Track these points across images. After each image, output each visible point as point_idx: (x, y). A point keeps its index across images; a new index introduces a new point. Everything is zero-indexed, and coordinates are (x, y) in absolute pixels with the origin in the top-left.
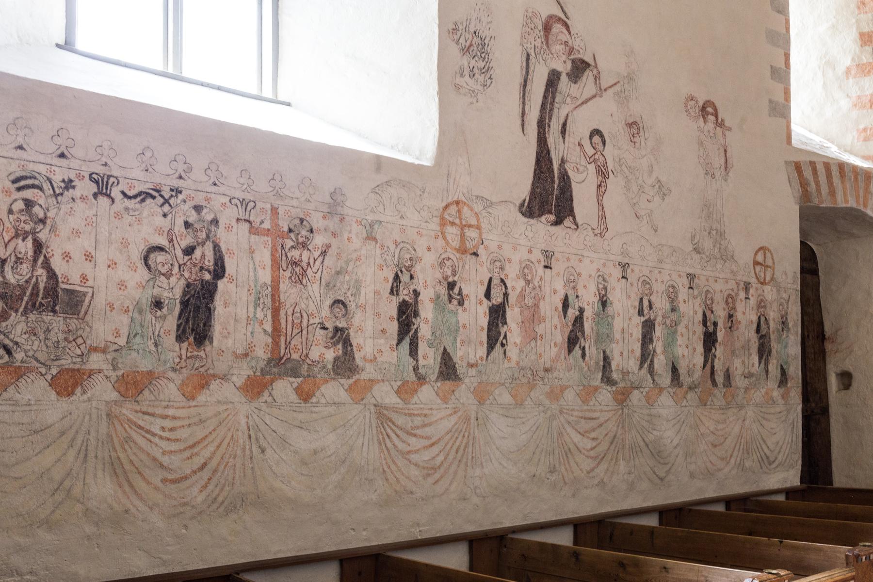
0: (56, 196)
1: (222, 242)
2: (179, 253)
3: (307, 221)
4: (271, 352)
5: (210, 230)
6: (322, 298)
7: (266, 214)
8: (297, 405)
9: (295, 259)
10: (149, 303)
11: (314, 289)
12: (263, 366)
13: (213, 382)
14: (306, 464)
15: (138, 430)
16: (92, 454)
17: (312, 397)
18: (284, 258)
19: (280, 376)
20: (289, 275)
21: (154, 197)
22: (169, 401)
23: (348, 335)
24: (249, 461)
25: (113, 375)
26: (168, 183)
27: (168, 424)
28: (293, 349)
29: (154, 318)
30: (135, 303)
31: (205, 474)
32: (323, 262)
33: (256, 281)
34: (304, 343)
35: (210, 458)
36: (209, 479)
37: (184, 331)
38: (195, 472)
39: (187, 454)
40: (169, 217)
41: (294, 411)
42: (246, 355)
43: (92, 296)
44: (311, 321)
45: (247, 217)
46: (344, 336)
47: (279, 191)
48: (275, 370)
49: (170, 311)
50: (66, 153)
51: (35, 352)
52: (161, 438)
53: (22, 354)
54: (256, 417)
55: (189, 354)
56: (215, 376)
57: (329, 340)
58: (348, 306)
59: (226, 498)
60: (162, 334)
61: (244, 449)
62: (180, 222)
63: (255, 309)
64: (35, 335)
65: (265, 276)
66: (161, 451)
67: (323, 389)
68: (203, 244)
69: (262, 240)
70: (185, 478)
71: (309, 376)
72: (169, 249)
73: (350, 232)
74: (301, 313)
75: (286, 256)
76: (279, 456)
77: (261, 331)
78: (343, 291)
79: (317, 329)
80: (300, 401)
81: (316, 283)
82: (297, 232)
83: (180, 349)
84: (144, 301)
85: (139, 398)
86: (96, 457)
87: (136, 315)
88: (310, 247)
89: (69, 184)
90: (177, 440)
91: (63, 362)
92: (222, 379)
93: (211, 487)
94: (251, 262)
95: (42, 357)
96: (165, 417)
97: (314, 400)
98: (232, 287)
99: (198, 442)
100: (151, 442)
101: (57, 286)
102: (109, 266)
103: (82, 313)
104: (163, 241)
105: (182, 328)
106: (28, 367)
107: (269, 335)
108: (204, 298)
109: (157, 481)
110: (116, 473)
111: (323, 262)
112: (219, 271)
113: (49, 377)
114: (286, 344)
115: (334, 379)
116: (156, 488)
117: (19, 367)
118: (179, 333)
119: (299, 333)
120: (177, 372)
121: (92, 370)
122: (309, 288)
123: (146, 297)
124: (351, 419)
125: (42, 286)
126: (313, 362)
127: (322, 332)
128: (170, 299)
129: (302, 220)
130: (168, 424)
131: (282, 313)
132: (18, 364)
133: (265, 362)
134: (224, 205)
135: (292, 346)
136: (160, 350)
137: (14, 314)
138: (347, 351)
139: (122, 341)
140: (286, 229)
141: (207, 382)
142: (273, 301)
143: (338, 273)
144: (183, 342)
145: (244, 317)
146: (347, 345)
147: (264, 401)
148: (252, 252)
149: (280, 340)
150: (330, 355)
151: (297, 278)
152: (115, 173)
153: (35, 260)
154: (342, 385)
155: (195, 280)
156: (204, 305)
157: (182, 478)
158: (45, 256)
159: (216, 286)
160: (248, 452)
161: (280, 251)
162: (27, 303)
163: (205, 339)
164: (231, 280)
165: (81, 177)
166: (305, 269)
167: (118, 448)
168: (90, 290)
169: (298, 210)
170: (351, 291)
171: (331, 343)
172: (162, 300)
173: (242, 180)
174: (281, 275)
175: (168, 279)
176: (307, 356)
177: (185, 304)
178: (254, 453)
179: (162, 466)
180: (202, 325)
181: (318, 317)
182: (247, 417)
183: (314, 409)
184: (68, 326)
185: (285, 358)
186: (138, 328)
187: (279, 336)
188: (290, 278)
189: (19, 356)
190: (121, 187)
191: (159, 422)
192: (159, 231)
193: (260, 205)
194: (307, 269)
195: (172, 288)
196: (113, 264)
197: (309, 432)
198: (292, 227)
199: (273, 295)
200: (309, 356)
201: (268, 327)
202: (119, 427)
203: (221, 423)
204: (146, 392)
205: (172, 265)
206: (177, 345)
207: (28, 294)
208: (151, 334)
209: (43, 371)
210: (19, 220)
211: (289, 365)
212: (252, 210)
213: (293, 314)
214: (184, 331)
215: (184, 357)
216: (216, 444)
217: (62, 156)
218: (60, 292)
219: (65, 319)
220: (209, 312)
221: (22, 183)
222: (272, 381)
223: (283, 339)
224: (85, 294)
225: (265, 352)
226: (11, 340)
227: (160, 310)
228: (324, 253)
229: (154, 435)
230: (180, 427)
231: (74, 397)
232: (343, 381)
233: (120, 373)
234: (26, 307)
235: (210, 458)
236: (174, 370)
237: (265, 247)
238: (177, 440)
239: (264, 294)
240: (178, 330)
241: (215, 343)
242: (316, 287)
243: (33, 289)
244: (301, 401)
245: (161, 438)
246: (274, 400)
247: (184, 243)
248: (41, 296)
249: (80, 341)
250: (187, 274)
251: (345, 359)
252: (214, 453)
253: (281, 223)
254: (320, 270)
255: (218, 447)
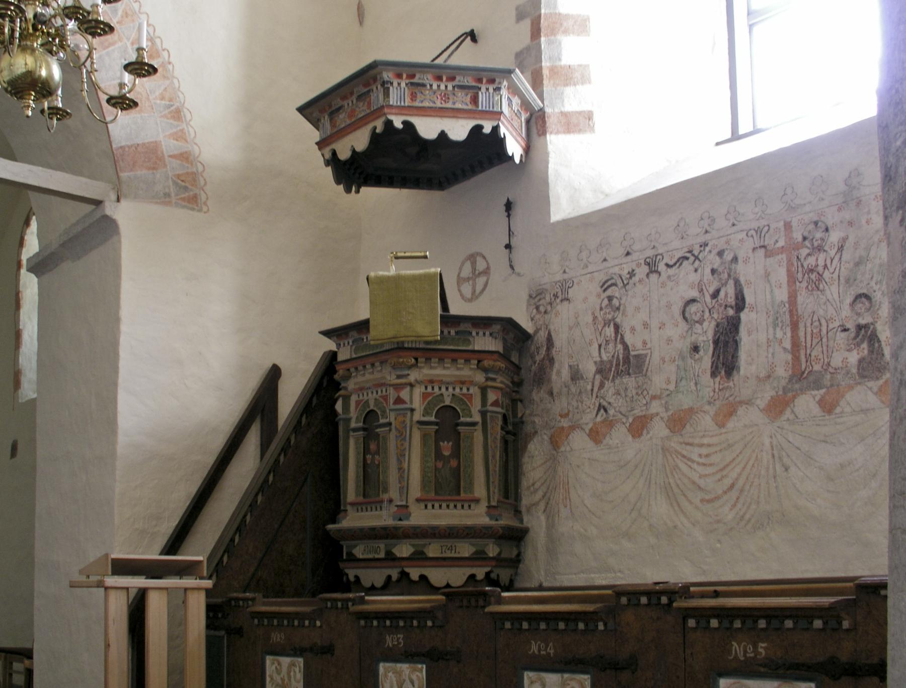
0: (625, 286)
1: (741, 276)
2: (708, 299)
3: (822, 221)
4: (792, 369)
5: (730, 269)
6: (841, 298)
7: (780, 232)
8: (820, 418)
9: (812, 266)
10: (688, 350)
11: (832, 291)
12: (785, 385)
13: (740, 408)
14: (832, 480)
15: (683, 459)
16: (653, 482)
17: (836, 407)
18: (800, 269)
19: (802, 391)
20: (806, 284)
21: (687, 258)
22: (705, 431)
23: (875, 330)
24: (773, 480)
25: (665, 415)
26: (694, 242)
27: (704, 451)
28: (814, 361)
29: (693, 361)
30: (679, 353)
31: (734, 494)
32: (840, 259)
33: (773, 302)
34: (825, 352)
35: (737, 479)
36: (738, 499)
37: (717, 367)
38: (725, 492)
39: (718, 476)
40: (699, 271)
41: (817, 425)
42: (769, 377)
43: (651, 356)
44: (831, 326)
45: (762, 244)
46: (869, 333)
47: (791, 204)
48: (797, 386)
49: (706, 351)
50: (630, 251)
51: (620, 407)
52: (698, 464)
53: (613, 410)
54: (779, 437)
55: (721, 387)
56: (741, 403)
57: (851, 341)
58: (872, 297)
59: (753, 516)
60: (700, 374)
61: (768, 469)
62: (708, 271)
63: (775, 329)
64: (619, 394)
65: (782, 295)
66: (698, 475)
67: (848, 396)
68: (726, 284)
69: (776, 260)
70: (718, 498)
71: (832, 385)
72: (700, 298)
73: (869, 213)
74: (819, 320)
75: (802, 266)
76: (804, 473)
77: (782, 350)
78: (865, 283)
79: (838, 333)
80: (823, 414)
81: (833, 284)
82: (811, 237)
83: (714, 383)
84: (685, 349)
85: (683, 432)
86: (656, 483)
87: (681, 363)
88: (826, 248)
89: (632, 274)
90: (711, 465)
91: (635, 412)
92: (747, 404)
93: (739, 506)
94: (768, 286)
95: (623, 410)
96: (701, 445)
97: (838, 410)
98: (753, 315)
99: (727, 465)
100: (691, 468)
101: (629, 353)
102: (660, 328)
103: (644, 372)
104: (694, 294)
105: (715, 365)
106: (616, 420)
107: (789, 352)
108: (731, 333)
109: (697, 501)
110: (668, 495)
111: (840, 259)
112: (740, 304)
113: (628, 425)
114: (806, 357)
115: (860, 383)
116: (697, 508)
117: (612, 420)
118: (713, 369)
119: (818, 342)
120: (712, 405)
121: (652, 415)
122: (828, 292)
123: (685, 345)
124: (883, 426)
125: (621, 356)
126: (835, 369)
127: (844, 335)
128: (704, 341)
129: (816, 223)
130: (704, 451)
131: (801, 325)
132: (611, 418)
133: (787, 380)
134: (741, 241)
135: (813, 358)
136: (698, 389)
137: (607, 383)
138: (874, 348)
139: (672, 387)
140: (800, 239)
141: (734, 409)
142: (791, 316)
143: (857, 264)
144: (716, 377)
145: (765, 340)
146: (874, 342)
147: (786, 419)
148: (767, 275)
149: (799, 353)
150: (853, 358)
151: (814, 286)
152: (660, 251)
153: (616, 339)
154: (870, 389)
155: (722, 319)
156: (731, 339)
157: (716, 498)
158: (621, 334)
159: (739, 319)
160: (771, 471)
161: (795, 264)
162: (614, 372)
163: (733, 370)
164: (752, 309)
165: (639, 265)
166: (821, 273)
167: (669, 475)
168: (649, 351)
169: (811, 215)
170: (874, 279)
171: (854, 344)
172: (698, 345)
173: (756, 210)
174: (797, 288)
175: (701, 324)
176: (829, 364)
177: (716, 342)
178: (777, 473)
179: (700, 488)
180: (730, 358)
181: (837, 320)
182: (771, 437)
183: (838, 420)
184: (637, 383)
185: (806, 372)
186: (683, 373)
187: (798, 351)
188: (807, 287)
189: (611, 412)
190: (665, 261)
191: (697, 450)
192: (692, 286)
193: (773, 226)
194: (823, 273)
195: (706, 332)
196: (662, 326)
197: (834, 445)
198: (806, 234)
199: (791, 311)
200: (831, 364)
201: (788, 344)
202: (669, 458)
203: (746, 446)
204: (688, 426)
205: (703, 312)
206: (712, 380)
207: (614, 366)
208: (692, 376)
209: (624, 420)
210: (605, 314)
211: (811, 378)
212: (766, 235)
213: (812, 324)
214: (717, 367)
215: (717, 390)
216: (742, 465)
217: (628, 254)
218: (631, 358)
219: (636, 377)
220: (736, 344)
221: (606, 286)
222: (794, 397)
223: (802, 353)
224: (646, 356)
225: (785, 370)
226: (607, 402)
227: (698, 353)
228: (841, 249)
229: (693, 461)
230: (714, 453)
231: (642, 438)
232: (871, 384)
233: (670, 413)
234: (614, 376)
235: (737, 479)
236: (709, 403)
237: (780, 266)
238: (711, 465)
239: (782, 313)
240: (712, 367)
241: (742, 372)
242: (834, 289)
243: (616, 361)
244: (826, 414)
245: (698, 464)
246: (797, 417)
247: (712, 290)
248: (621, 365)
249: (645, 393)
250: (715, 316)
251: (871, 358)
252: (740, 474)
253: (795, 235)
254: (837, 270)
255: (744, 468)
